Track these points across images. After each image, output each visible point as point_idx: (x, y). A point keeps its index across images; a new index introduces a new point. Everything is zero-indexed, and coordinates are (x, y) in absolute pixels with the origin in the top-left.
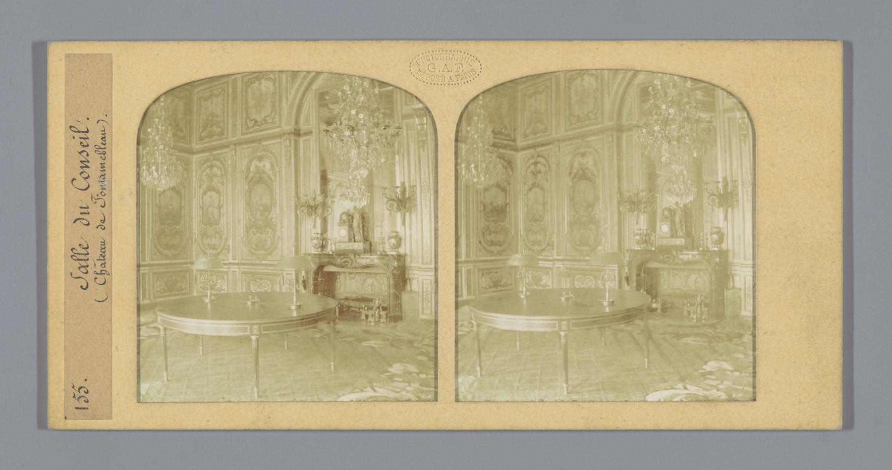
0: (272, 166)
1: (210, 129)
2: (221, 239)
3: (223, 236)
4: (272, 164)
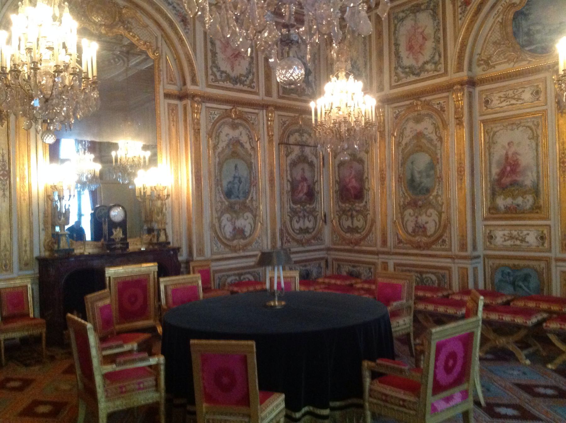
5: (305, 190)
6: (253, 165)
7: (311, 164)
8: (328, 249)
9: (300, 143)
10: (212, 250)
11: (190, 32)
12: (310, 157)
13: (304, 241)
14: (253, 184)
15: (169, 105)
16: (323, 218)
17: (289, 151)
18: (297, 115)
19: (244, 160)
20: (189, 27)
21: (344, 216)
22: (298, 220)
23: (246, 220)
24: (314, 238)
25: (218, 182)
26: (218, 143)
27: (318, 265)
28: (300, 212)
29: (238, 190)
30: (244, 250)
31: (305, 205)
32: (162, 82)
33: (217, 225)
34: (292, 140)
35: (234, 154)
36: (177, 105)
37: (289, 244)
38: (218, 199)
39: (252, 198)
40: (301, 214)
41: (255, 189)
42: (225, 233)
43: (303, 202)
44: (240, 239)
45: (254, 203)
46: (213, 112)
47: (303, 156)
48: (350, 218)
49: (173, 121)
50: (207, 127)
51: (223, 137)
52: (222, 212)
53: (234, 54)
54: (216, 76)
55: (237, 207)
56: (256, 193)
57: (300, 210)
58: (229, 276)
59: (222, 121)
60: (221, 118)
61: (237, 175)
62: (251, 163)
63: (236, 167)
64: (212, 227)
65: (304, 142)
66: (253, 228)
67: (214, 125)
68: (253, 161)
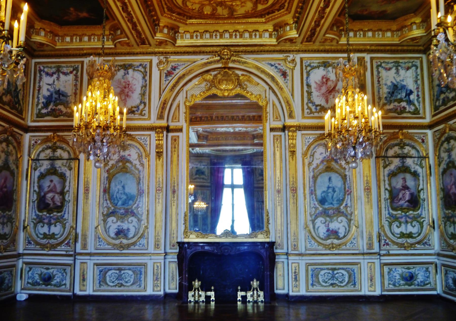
0: (140, 156)
1: (54, 107)
2: (64, 228)
3: (67, 224)
4: (139, 154)
5: (407, 197)
6: (348, 177)
7: (415, 175)
8: (438, 255)
9: (400, 155)
10: (306, 247)
11: (289, 82)
12: (413, 167)
13: (406, 245)
14: (348, 193)
15: (274, 136)
16: (431, 224)
17: (387, 163)
18: (397, 131)
19: (338, 173)
20: (288, 78)
21: (448, 222)
22: (398, 225)
23: (340, 223)
24: (418, 243)
25: (312, 192)
26: (313, 161)
27: (424, 269)
28: (402, 218)
29: (332, 197)
30: (339, 250)
31: (407, 212)
32: (268, 121)
33: (311, 226)
34: (391, 153)
35: (329, 169)
36: (281, 135)
37: (388, 247)
38: (312, 206)
39: (346, 205)
40: (403, 220)
41: (349, 197)
42: (319, 234)
43: (405, 209)
44: (334, 239)
45: (349, 209)
46: (308, 137)
47: (403, 166)
48: (452, 225)
49: (277, 147)
50: (302, 149)
51: (317, 155)
52: (316, 216)
53: (328, 90)
54: (311, 109)
55: (331, 212)
56: (351, 200)
57: (400, 216)
58: (322, 269)
59: (316, 144)
60: (315, 141)
61: (331, 185)
62: (346, 176)
63: (330, 179)
64: (306, 227)
65: (404, 154)
66: (347, 231)
67: (309, 147)
68: (347, 173)
